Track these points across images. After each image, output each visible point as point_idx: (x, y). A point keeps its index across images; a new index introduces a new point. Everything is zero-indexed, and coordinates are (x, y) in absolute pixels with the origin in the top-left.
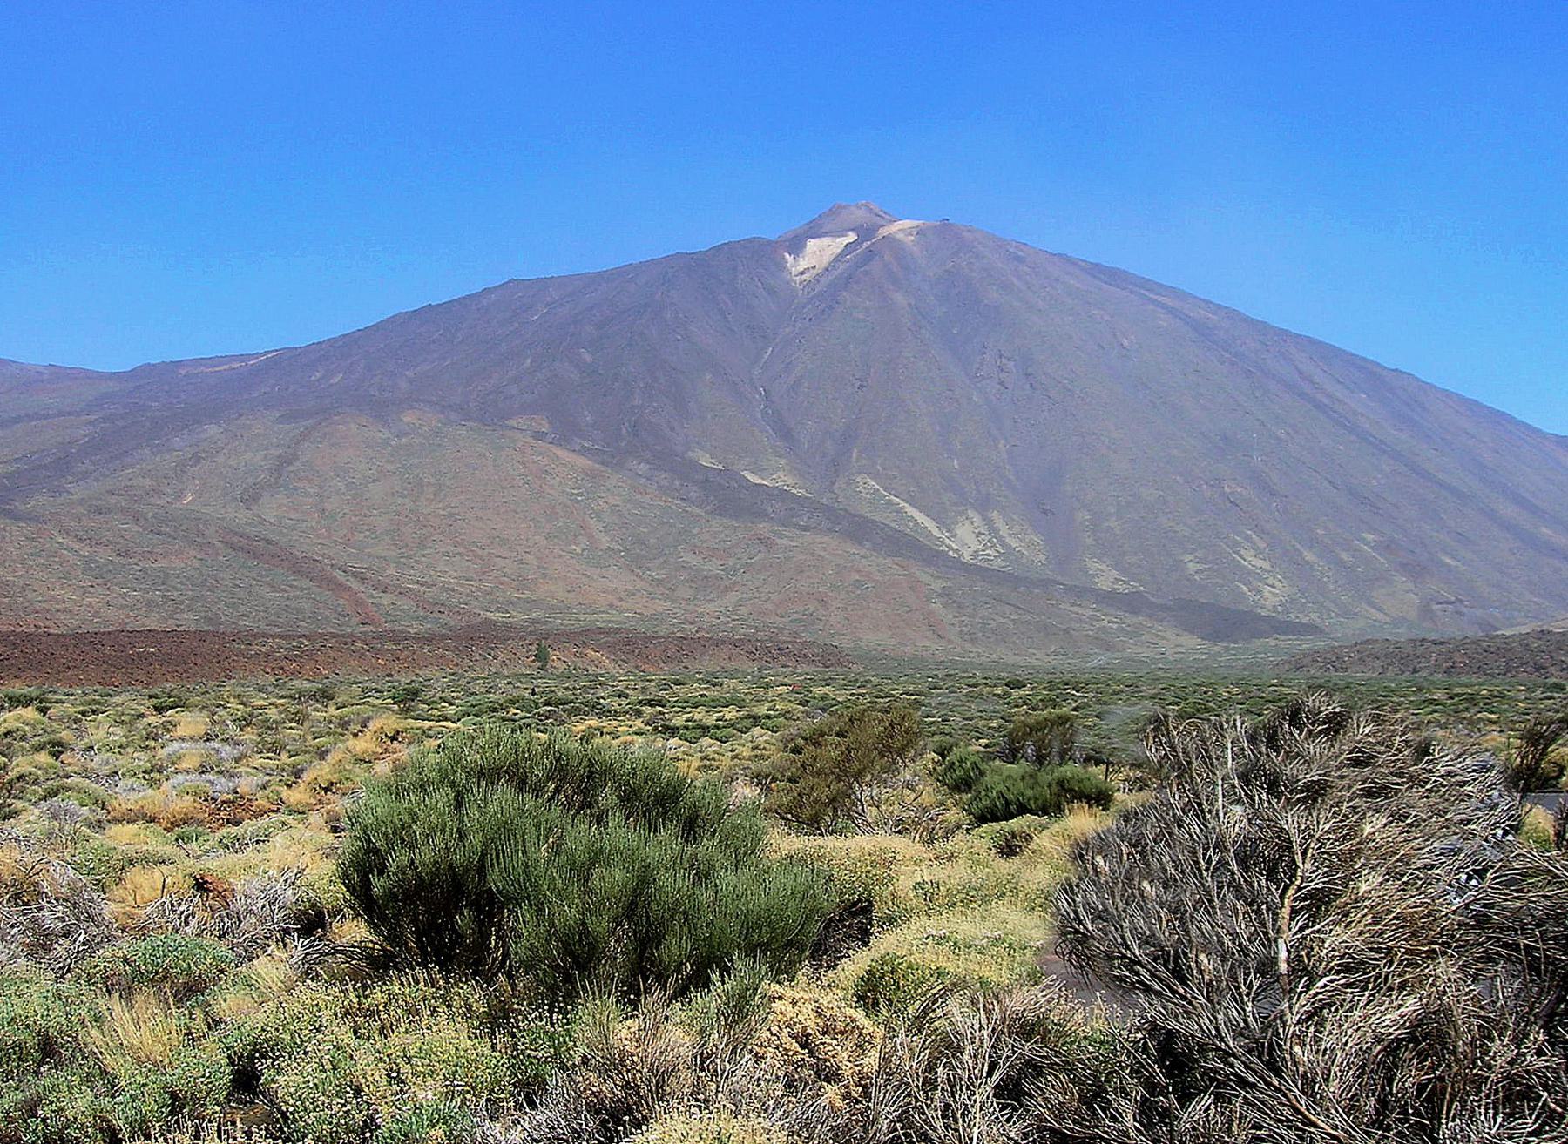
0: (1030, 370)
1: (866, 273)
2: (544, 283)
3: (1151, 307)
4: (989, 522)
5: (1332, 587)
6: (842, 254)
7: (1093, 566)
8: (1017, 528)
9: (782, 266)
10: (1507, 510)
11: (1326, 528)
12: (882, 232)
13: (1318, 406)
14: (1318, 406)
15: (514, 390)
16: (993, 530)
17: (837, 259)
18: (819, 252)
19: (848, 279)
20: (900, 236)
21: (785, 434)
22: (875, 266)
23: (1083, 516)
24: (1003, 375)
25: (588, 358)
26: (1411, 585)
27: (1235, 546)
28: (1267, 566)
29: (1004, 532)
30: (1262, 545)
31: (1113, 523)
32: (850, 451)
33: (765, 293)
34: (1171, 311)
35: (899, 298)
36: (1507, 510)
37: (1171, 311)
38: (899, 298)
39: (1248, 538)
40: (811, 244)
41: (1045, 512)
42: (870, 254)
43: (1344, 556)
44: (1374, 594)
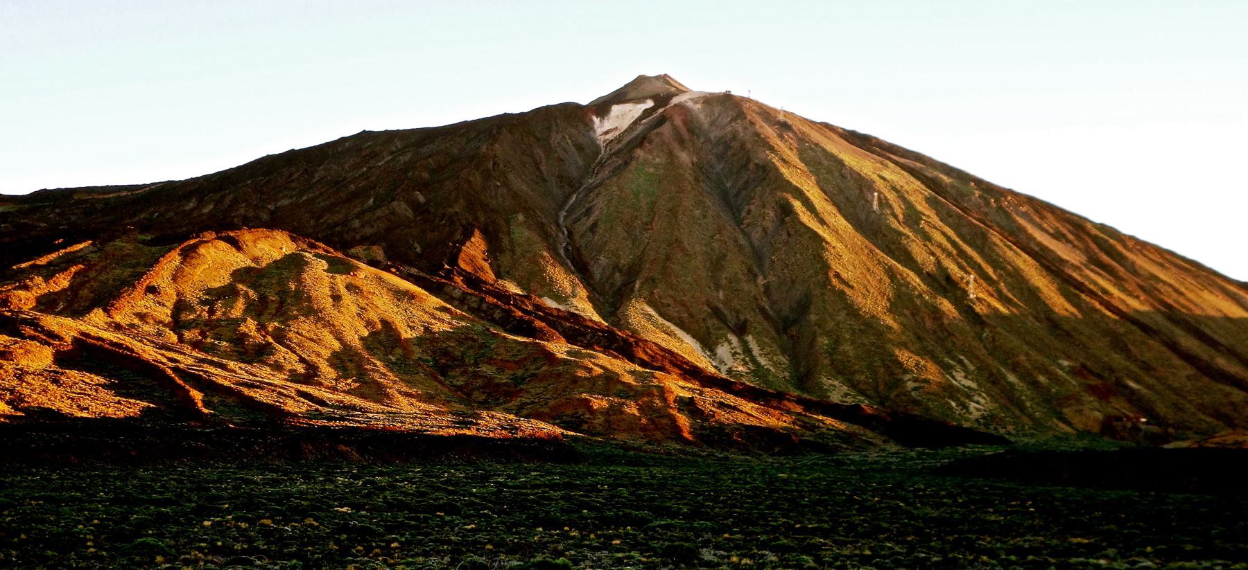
4: (745, 344)
5: (1028, 404)
6: (640, 119)
7: (826, 381)
8: (768, 349)
9: (589, 126)
10: (1188, 342)
11: (1027, 355)
12: (675, 101)
15: (356, 224)
16: (747, 351)
17: (635, 123)
19: (641, 141)
20: (690, 104)
22: (666, 129)
23: (823, 341)
26: (1096, 404)
27: (952, 367)
28: (974, 385)
29: (756, 351)
30: (972, 368)
33: (573, 149)
35: (684, 157)
36: (1188, 342)
38: (684, 157)
39: (960, 362)
40: (616, 109)
42: (662, 121)
43: (1042, 379)
44: (1065, 410)
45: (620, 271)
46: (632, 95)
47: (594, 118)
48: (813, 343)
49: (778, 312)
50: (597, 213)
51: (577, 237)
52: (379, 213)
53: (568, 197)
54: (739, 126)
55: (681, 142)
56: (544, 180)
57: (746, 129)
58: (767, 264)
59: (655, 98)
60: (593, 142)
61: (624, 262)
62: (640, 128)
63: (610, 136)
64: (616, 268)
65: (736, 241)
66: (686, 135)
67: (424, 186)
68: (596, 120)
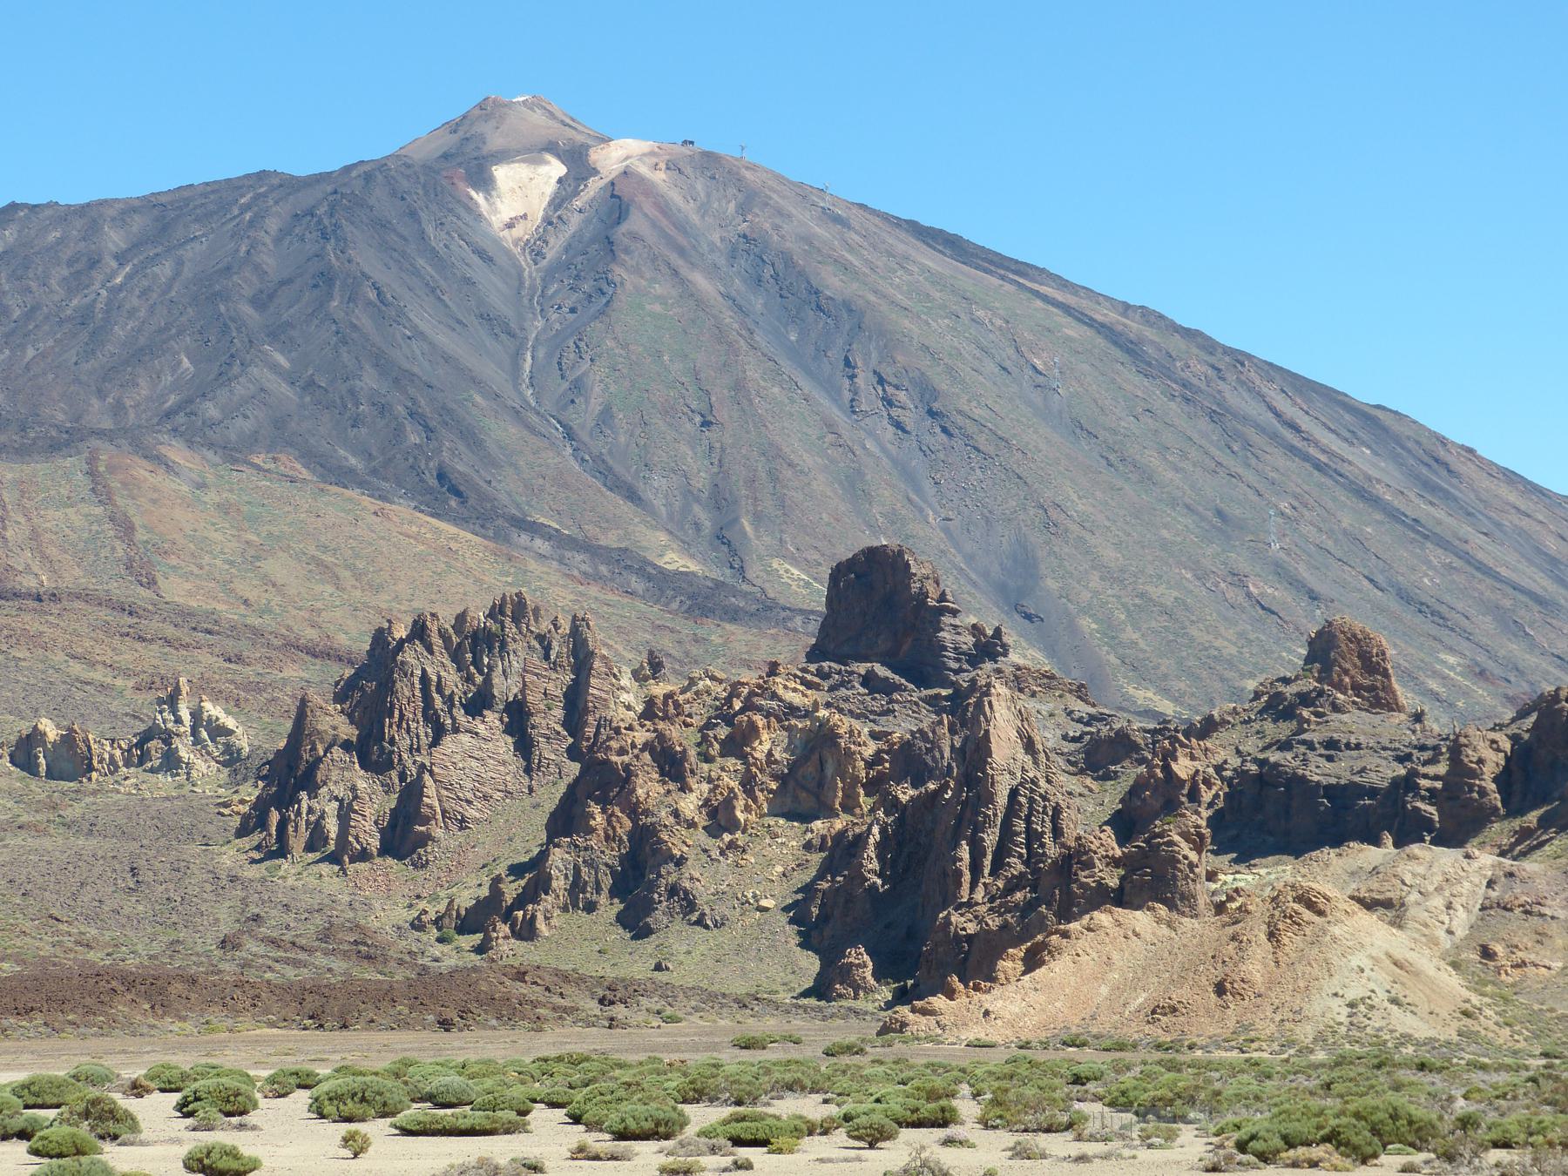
0: (936, 406)
1: (635, 237)
2: (90, 215)
3: (1039, 303)
13: (1318, 466)
14: (1318, 466)
15: (211, 410)
17: (559, 202)
18: (519, 195)
20: (643, 170)
21: (633, 496)
22: (636, 222)
23: (1087, 624)
24: (895, 412)
25: (281, 360)
31: (1130, 634)
32: (736, 520)
33: (476, 258)
34: (1067, 309)
35: (700, 280)
37: (1067, 309)
40: (501, 173)
41: (1028, 617)
43: (1433, 685)
45: (698, 500)
46: (495, 142)
47: (473, 193)
48: (1073, 629)
49: (986, 575)
50: (597, 389)
51: (586, 438)
52: (241, 389)
53: (517, 357)
54: (763, 221)
55: (681, 252)
56: (459, 322)
57: (777, 228)
58: (928, 485)
59: (551, 148)
60: (497, 242)
61: (701, 481)
62: (575, 220)
63: (518, 232)
64: (689, 494)
65: (864, 448)
66: (681, 240)
67: (275, 334)
68: (479, 198)
